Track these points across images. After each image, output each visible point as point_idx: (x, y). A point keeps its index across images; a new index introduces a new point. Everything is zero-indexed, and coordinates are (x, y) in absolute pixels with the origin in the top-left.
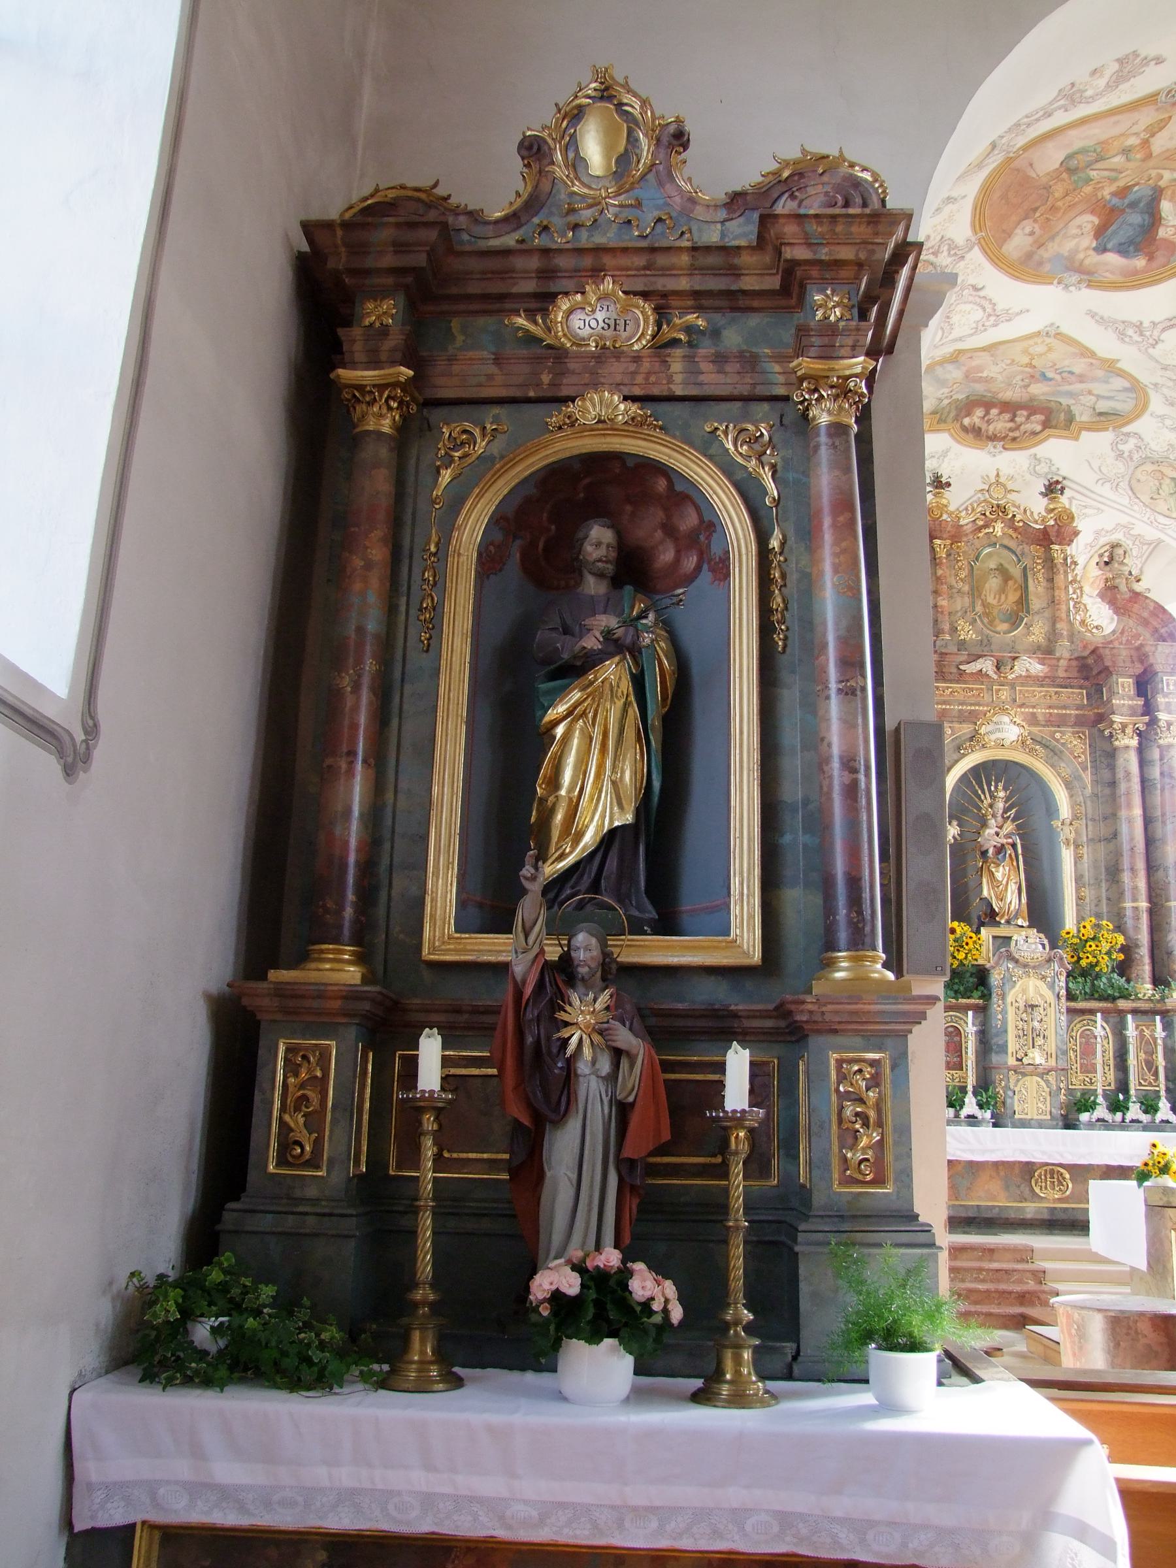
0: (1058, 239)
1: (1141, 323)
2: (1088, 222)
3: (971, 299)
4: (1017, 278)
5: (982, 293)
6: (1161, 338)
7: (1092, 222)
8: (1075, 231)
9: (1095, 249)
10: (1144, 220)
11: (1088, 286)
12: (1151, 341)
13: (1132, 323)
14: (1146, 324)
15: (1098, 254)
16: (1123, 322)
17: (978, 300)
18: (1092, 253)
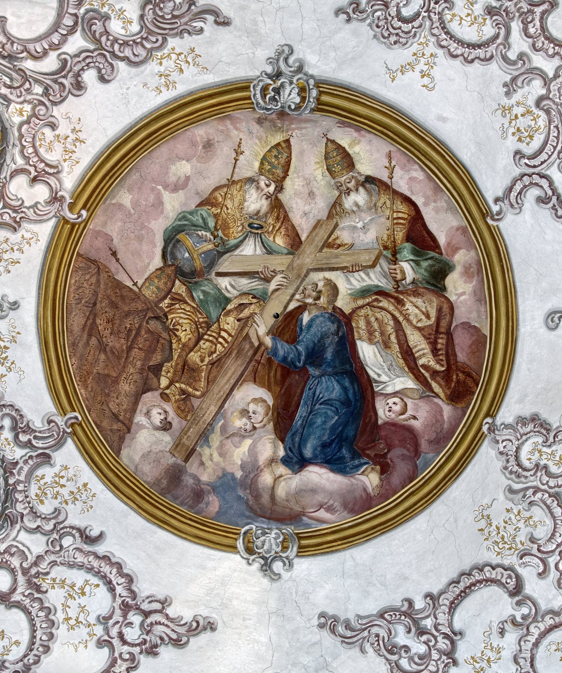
0: (215, 439)
1: (411, 603)
2: (255, 400)
3: (80, 558)
4: (162, 523)
5: (101, 549)
6: (457, 625)
7: (264, 401)
8: (239, 423)
9: (286, 461)
10: (345, 389)
11: (303, 551)
12: (443, 644)
13: (394, 610)
14: (419, 604)
15: (295, 472)
16: (381, 616)
17: (96, 564)
18: (282, 470)
